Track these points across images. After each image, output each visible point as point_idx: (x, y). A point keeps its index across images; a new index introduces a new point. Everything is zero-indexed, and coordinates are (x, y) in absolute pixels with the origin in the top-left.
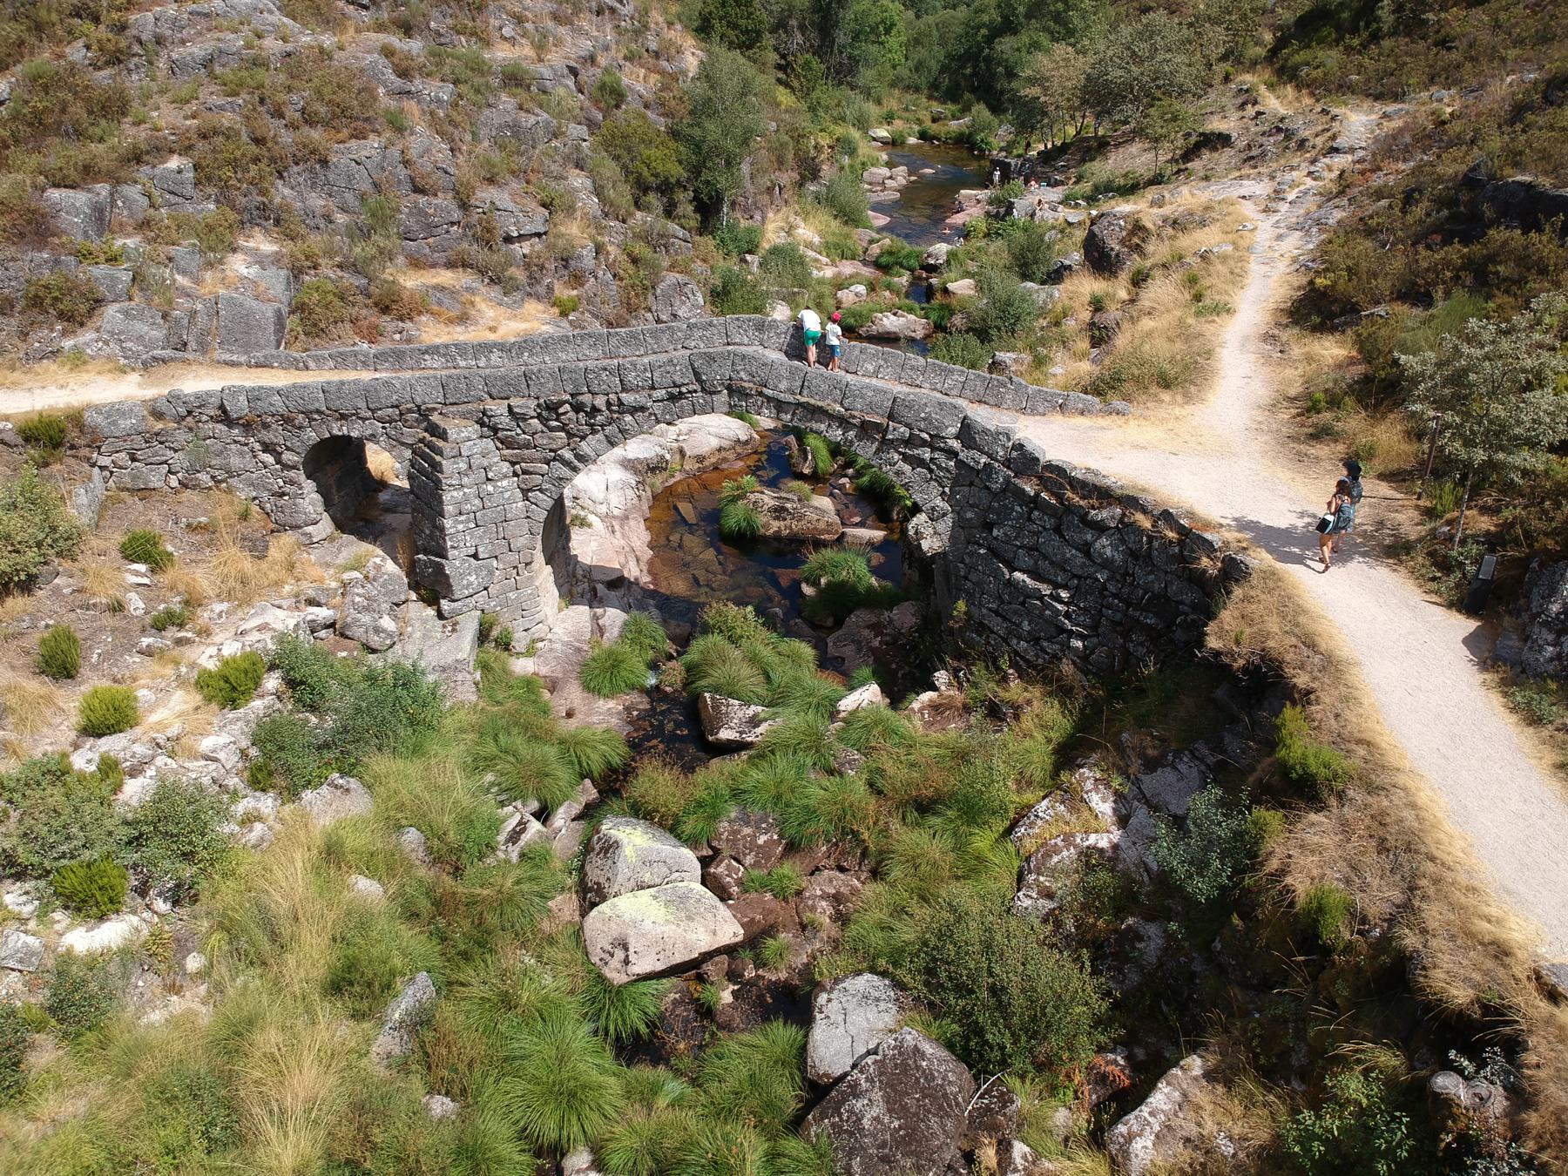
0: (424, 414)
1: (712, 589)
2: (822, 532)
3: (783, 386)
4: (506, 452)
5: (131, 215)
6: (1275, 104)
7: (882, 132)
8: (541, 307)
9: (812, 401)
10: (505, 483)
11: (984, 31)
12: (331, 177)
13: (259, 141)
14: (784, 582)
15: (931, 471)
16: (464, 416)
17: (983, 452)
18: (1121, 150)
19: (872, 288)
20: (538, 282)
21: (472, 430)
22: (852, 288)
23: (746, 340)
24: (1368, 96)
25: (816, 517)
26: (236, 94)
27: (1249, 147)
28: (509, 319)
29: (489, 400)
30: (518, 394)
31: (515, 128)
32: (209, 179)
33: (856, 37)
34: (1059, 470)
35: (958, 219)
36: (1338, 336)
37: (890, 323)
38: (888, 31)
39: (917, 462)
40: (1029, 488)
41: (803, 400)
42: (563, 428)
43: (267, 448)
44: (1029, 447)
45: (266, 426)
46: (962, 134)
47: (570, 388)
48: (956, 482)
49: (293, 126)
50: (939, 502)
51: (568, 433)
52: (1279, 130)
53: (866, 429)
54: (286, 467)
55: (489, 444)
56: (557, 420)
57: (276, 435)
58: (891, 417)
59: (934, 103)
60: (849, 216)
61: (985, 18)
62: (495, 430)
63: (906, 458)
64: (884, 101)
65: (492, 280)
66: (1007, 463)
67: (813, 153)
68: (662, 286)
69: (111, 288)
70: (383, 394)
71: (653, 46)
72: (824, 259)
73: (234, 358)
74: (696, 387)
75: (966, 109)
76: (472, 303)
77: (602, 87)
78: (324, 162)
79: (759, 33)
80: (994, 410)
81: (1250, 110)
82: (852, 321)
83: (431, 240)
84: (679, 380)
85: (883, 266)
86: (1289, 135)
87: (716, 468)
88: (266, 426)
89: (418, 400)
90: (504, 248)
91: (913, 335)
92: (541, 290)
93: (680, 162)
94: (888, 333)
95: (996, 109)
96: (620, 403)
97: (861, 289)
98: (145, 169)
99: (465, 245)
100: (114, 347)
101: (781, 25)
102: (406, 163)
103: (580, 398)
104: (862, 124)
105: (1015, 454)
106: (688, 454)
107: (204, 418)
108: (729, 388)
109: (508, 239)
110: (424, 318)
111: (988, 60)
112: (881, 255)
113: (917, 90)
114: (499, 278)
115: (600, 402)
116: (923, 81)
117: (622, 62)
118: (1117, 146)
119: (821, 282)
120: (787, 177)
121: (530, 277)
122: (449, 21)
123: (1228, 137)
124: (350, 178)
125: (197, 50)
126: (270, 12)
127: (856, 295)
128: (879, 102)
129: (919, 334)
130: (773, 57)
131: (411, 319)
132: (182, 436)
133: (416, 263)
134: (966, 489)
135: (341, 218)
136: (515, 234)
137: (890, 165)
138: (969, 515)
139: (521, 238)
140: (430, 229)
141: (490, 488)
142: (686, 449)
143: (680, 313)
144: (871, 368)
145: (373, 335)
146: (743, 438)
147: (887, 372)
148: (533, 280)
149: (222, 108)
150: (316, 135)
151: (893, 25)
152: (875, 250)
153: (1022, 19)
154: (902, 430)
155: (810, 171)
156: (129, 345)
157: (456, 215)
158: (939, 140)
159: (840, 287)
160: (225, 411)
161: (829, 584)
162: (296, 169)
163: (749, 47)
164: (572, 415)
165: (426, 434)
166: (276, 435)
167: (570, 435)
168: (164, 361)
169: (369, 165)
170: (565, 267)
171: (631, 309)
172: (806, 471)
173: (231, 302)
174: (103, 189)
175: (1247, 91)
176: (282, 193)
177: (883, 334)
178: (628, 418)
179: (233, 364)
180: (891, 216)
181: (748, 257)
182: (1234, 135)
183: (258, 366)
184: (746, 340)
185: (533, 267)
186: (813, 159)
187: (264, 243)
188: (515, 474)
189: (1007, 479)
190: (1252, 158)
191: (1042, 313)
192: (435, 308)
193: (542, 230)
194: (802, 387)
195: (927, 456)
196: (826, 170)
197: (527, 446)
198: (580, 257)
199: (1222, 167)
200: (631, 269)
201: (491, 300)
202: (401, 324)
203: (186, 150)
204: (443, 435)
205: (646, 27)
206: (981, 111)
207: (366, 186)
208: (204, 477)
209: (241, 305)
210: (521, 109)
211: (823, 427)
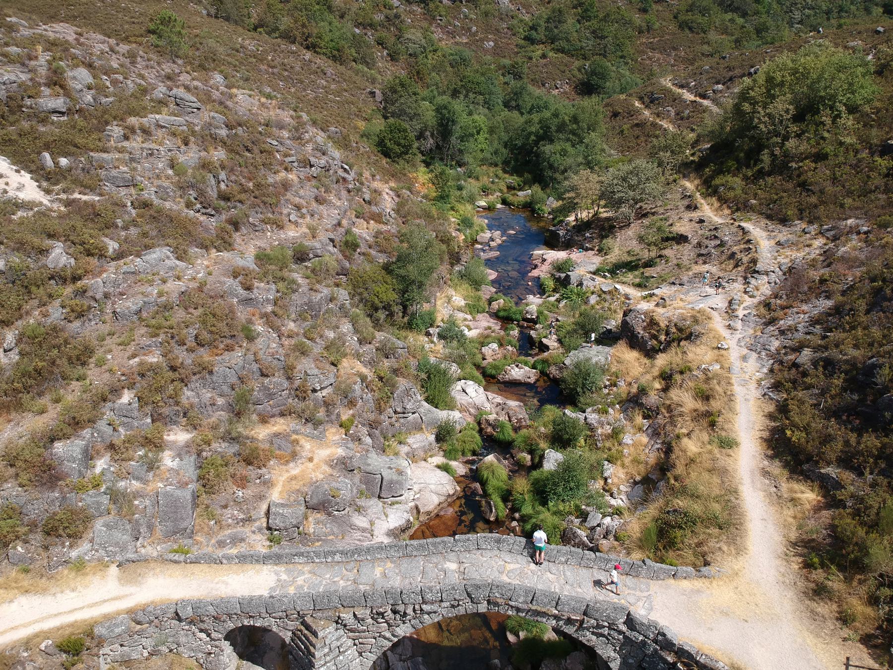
0: (301, 616)
1: (450, 633)
3: (521, 601)
4: (351, 634)
5: (103, 441)
6: (708, 210)
7: (483, 203)
8: (334, 430)
9: (539, 609)
10: (349, 652)
11: (533, 137)
12: (215, 378)
13: (173, 369)
14: (494, 626)
15: (608, 639)
16: (326, 619)
17: (640, 634)
18: (623, 232)
19: (501, 345)
21: (332, 627)
22: (490, 345)
23: (489, 547)
24: (762, 214)
26: (157, 335)
27: (699, 245)
28: (319, 448)
29: (342, 608)
30: (359, 605)
31: (310, 305)
32: (146, 404)
33: (462, 139)
34: (689, 655)
35: (535, 273)
36: (809, 483)
37: (517, 373)
38: (478, 133)
39: (599, 635)
40: (670, 659)
41: (534, 608)
42: (386, 622)
43: (201, 631)
44: (669, 636)
45: (202, 621)
46: (526, 202)
47: (391, 602)
48: (622, 646)
49: (191, 350)
50: (612, 654)
51: (388, 624)
52: (716, 237)
53: (569, 621)
54: (212, 639)
55: (341, 632)
56: (383, 618)
57: (209, 624)
58: (585, 614)
59: (507, 176)
60: (476, 284)
61: (533, 129)
62: (345, 626)
63: (593, 633)
64: (481, 178)
65: (306, 420)
66: (655, 641)
67: (457, 250)
69: (97, 509)
70: (276, 606)
71: (367, 197)
72: (469, 317)
73: (176, 558)
74: (468, 600)
75: (528, 184)
76: (297, 442)
77: (346, 243)
78: (211, 372)
79: (410, 146)
80: (636, 579)
81: (695, 215)
82: (494, 372)
83: (271, 402)
84: (457, 597)
85: (505, 319)
86: (722, 244)
87: (437, 515)
88: (202, 621)
89: (298, 609)
91: (529, 380)
93: (394, 290)
95: (544, 187)
96: (421, 610)
97: (495, 346)
98: (109, 404)
99: (290, 400)
100: (102, 552)
101: (420, 136)
102: (256, 361)
103: (398, 608)
104: (472, 200)
105: (660, 638)
107: (165, 619)
108: (489, 602)
109: (314, 391)
110: (272, 463)
111: (538, 155)
112: (499, 311)
113: (496, 165)
115: (410, 611)
116: (499, 160)
117: (355, 220)
118: (621, 228)
119: (472, 341)
120: (444, 269)
121: (327, 411)
122: (260, 216)
123: (686, 237)
124: (225, 377)
125: (130, 304)
126: (168, 258)
128: (477, 179)
129: (532, 380)
130: (420, 157)
131: (264, 466)
132: (151, 630)
133: (264, 420)
134: (629, 648)
135: (220, 401)
137: (490, 227)
138: (631, 661)
139: (322, 389)
140: (271, 396)
141: (341, 658)
143: (408, 407)
144: (563, 560)
145: (243, 482)
146: (451, 492)
147: (573, 561)
148: (329, 413)
149: (149, 346)
150: (205, 355)
151: (481, 129)
152: (495, 305)
154: (593, 621)
155: (455, 259)
156: (110, 548)
157: (286, 384)
159: (483, 344)
160: (177, 614)
161: (526, 640)
162: (194, 378)
163: (407, 153)
164: (392, 616)
165: (303, 628)
166: (209, 624)
167: (389, 625)
168: (133, 562)
169: (236, 368)
171: (380, 410)
172: (492, 519)
173: (166, 494)
174: (86, 433)
175: (689, 197)
176: (188, 395)
178: (426, 616)
179: (176, 562)
180: (497, 271)
181: (431, 330)
182: (690, 236)
183: (191, 563)
184: (489, 547)
185: (327, 404)
186: (457, 253)
187: (179, 436)
188: (355, 644)
189: (656, 650)
190: (702, 255)
191: (604, 370)
192: (278, 452)
194: (532, 600)
195: (606, 633)
196: (464, 258)
197: (364, 631)
198: (354, 391)
199: (686, 257)
200: (380, 384)
202: (259, 471)
203: (131, 386)
204: (315, 634)
205: (362, 184)
206: (536, 188)
207: (234, 380)
208: (164, 649)
209: (172, 495)
210: (311, 289)
211: (544, 620)
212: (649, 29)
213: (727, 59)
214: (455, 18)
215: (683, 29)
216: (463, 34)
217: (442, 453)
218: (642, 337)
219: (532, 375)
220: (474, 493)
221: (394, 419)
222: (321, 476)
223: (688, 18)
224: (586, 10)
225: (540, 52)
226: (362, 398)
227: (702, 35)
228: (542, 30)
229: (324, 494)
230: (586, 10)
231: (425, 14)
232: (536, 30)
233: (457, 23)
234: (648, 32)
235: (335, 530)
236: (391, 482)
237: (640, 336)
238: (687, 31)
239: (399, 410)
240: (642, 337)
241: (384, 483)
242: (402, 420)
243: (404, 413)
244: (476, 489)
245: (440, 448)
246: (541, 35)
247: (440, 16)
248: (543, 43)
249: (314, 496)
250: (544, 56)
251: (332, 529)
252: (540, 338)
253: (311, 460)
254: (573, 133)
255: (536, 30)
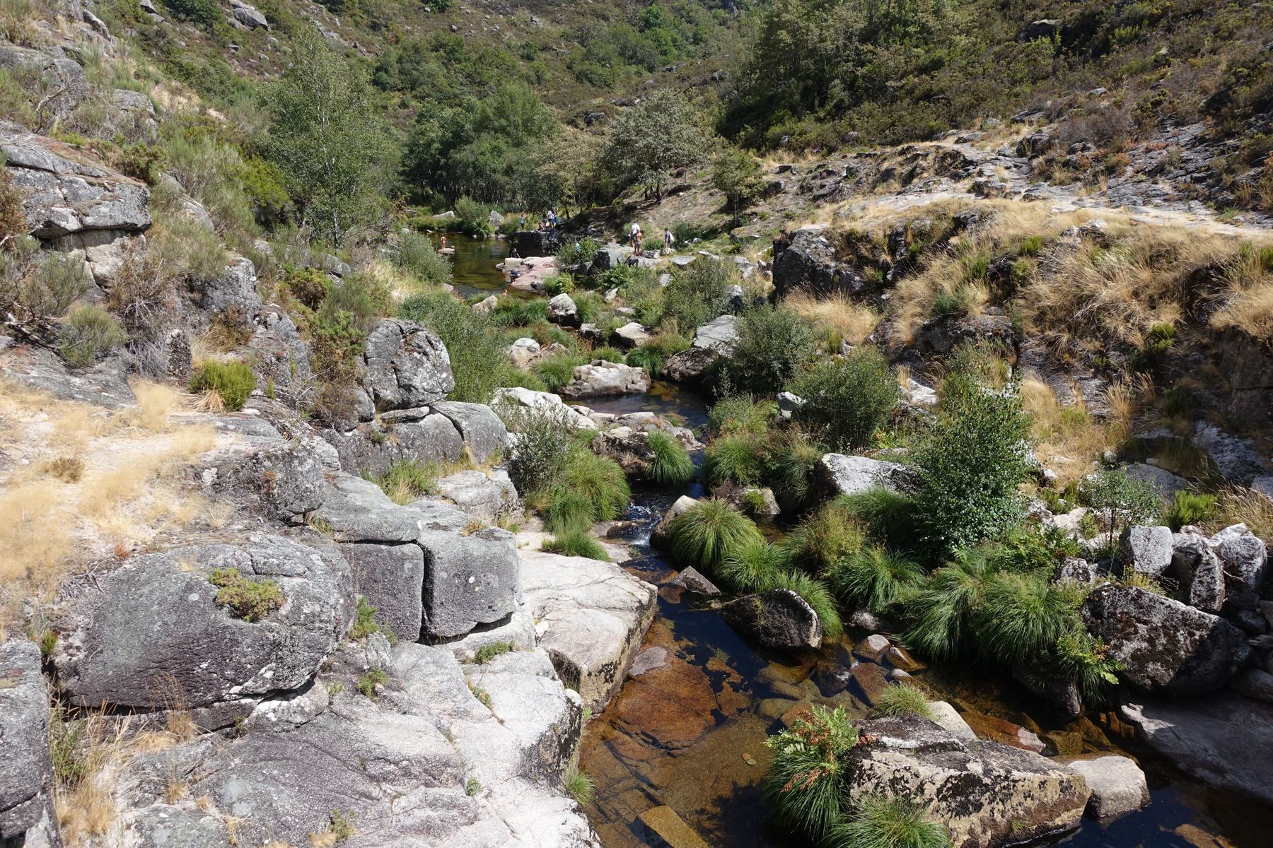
2: (1054, 810)
11: (437, 145)
20: (150, 337)
25: (1038, 778)
68: (375, 337)
90: (42, 259)
92: (162, 356)
94: (608, 389)
106: (585, 668)
114: (42, 329)
127: (529, 349)
136: (73, 224)
139: (87, 234)
142: (571, 655)
143: (417, 382)
153: (472, 134)
158: (432, 229)
170: (201, 305)
177: (601, 390)
193: (140, 220)
198: (232, 282)
201: (32, 387)
212: (539, 79)
213: (674, 71)
214: (258, 48)
215: (581, 82)
216: (276, 71)
217: (535, 521)
218: (838, 272)
219: (637, 378)
220: (691, 595)
221: (376, 424)
222: (148, 535)
223: (585, 67)
224: (452, 51)
225: (396, 101)
226: (265, 324)
227: (606, 89)
228: (395, 69)
229: (182, 606)
230: (452, 51)
231: (207, 39)
232: (386, 71)
233: (263, 56)
234: (539, 83)
235: (284, 801)
236: (465, 568)
237: (831, 271)
238: (588, 84)
239: (389, 394)
240: (838, 272)
241: (440, 575)
242: (403, 428)
243: (405, 405)
244: (691, 583)
245: (528, 506)
246: (394, 79)
247: (234, 43)
248: (399, 90)
249: (115, 633)
250: (404, 105)
251: (264, 803)
252: (612, 329)
253: (69, 470)
254: (502, 130)
255: (386, 71)
